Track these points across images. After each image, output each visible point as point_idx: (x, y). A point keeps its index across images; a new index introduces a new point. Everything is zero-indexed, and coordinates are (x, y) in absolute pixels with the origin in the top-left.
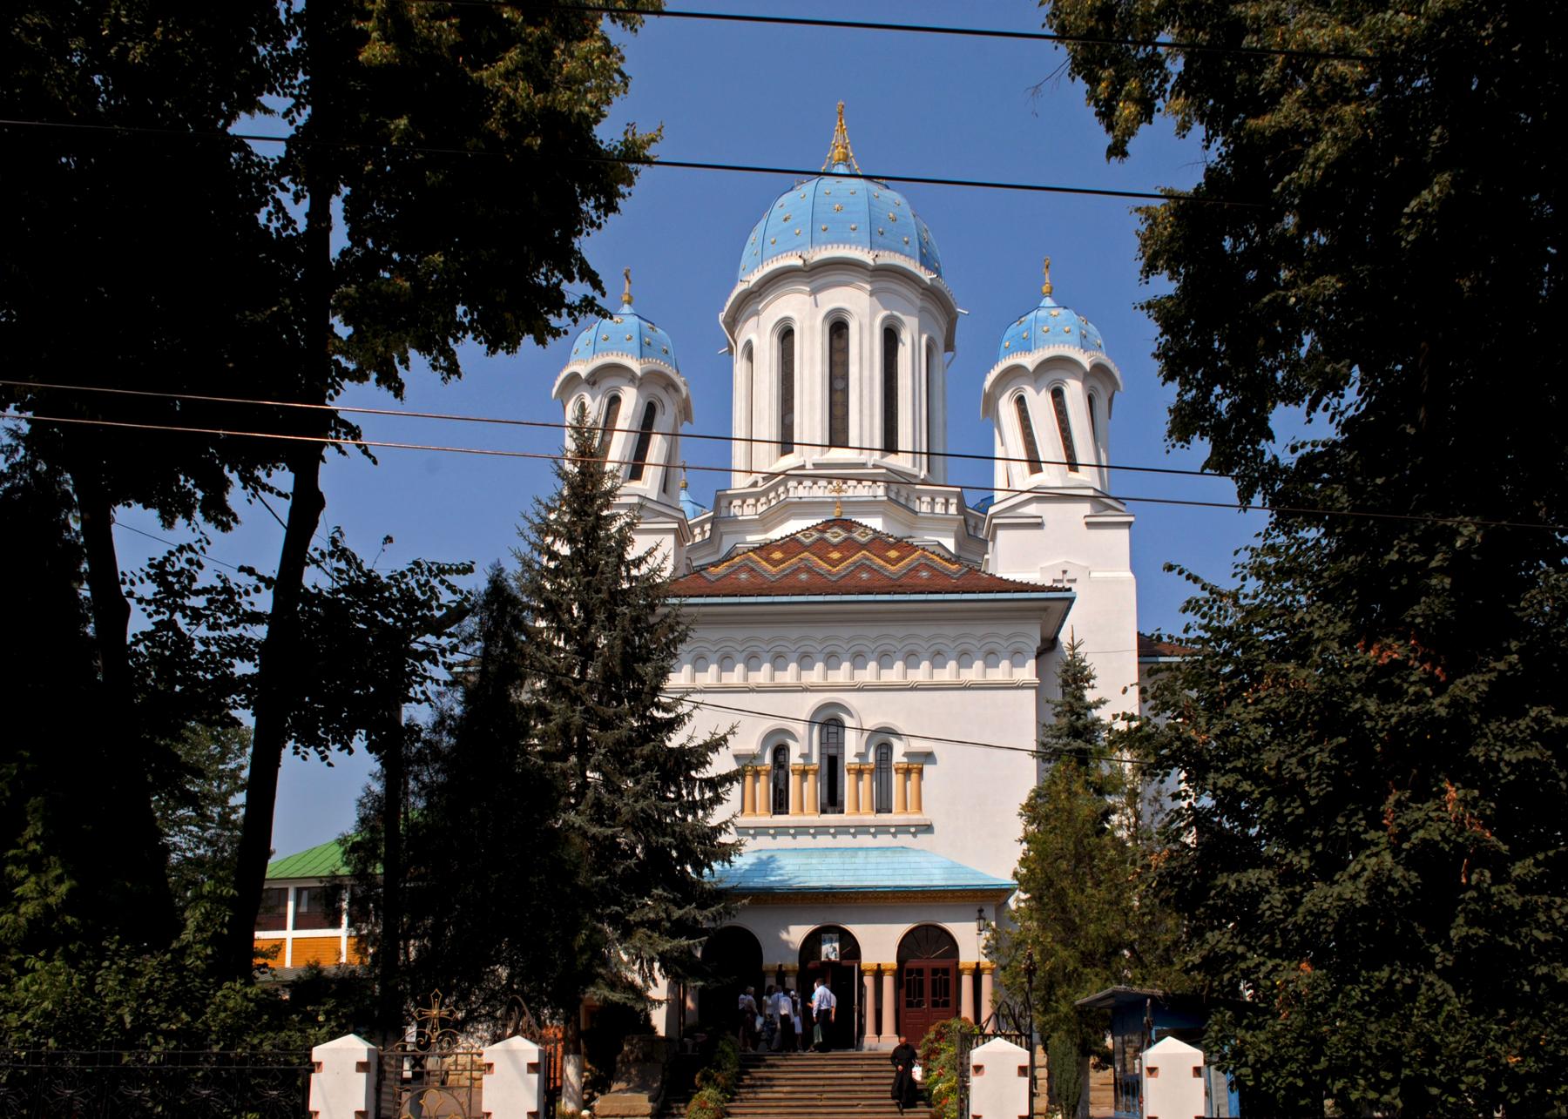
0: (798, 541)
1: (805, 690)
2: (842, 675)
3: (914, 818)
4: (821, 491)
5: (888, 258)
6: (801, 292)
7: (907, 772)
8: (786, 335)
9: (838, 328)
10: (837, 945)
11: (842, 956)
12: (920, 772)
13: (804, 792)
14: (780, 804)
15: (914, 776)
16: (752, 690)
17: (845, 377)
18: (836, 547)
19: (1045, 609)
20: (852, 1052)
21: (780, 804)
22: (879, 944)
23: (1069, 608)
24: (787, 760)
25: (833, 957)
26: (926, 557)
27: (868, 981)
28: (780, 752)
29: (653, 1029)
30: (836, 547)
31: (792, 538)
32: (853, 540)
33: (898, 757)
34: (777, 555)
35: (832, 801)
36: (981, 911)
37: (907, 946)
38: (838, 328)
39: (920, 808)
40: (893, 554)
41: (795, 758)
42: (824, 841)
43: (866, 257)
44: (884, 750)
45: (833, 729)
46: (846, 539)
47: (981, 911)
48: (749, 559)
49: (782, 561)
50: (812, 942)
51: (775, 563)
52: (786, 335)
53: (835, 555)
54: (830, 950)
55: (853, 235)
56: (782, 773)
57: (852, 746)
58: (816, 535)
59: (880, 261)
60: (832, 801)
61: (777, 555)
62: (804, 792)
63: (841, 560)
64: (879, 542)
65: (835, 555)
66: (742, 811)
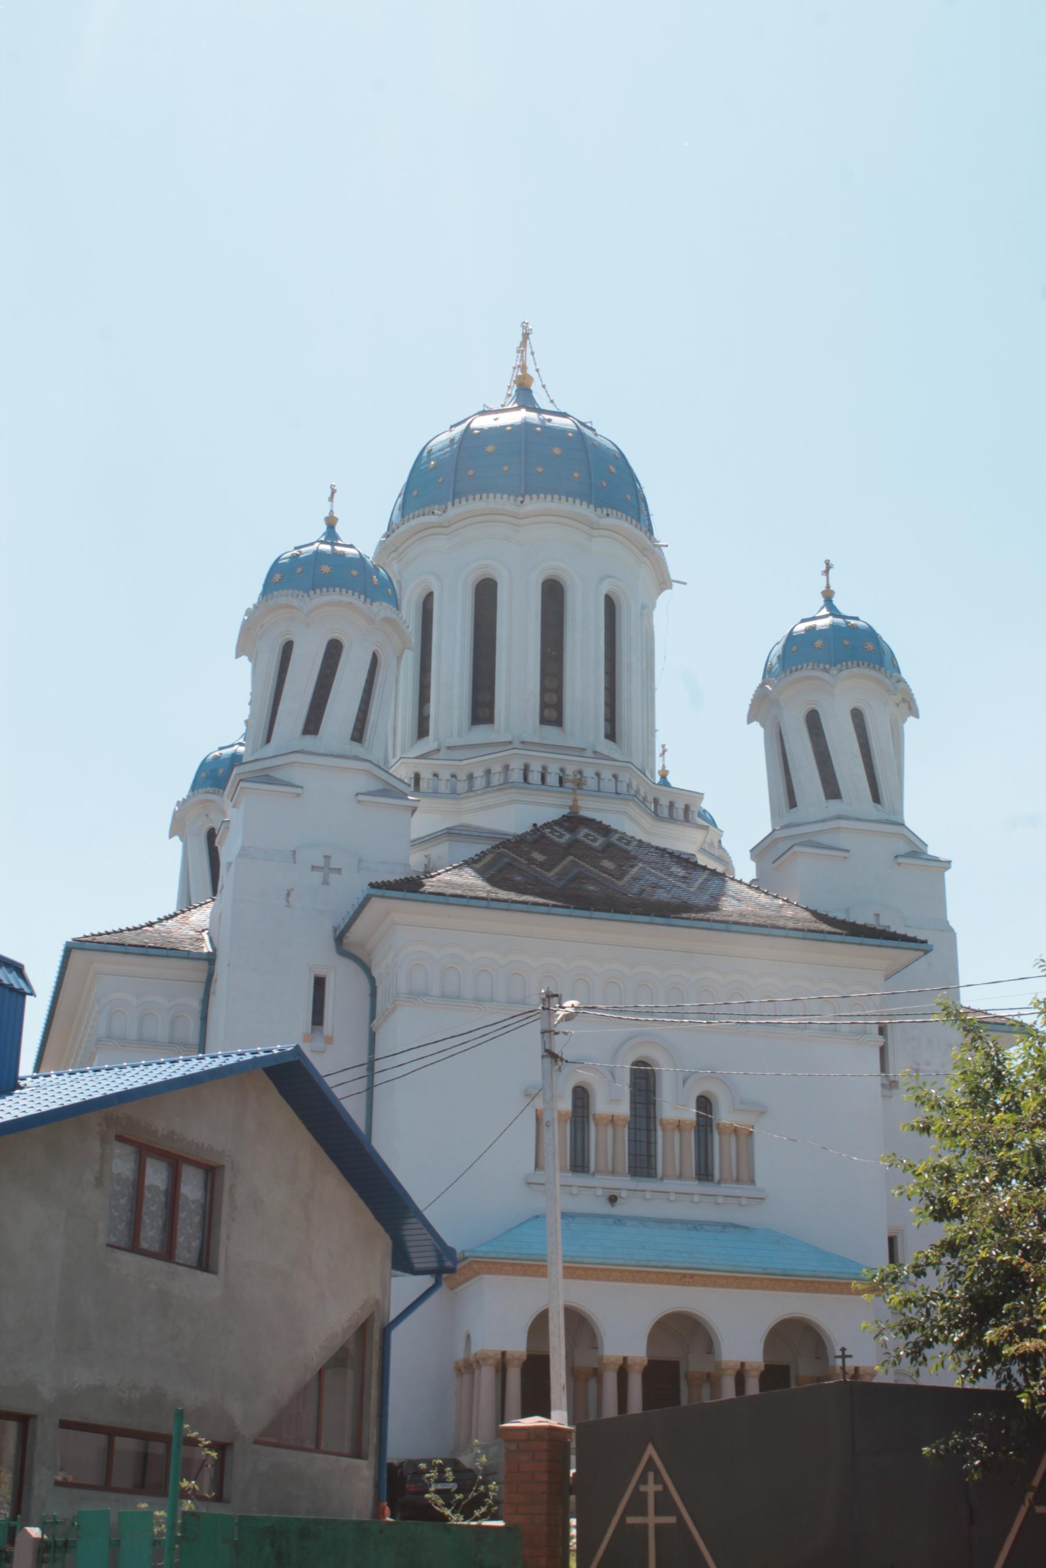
9: (553, 595)
33: (725, 1115)
38: (553, 595)
39: (752, 1181)
44: (704, 1103)
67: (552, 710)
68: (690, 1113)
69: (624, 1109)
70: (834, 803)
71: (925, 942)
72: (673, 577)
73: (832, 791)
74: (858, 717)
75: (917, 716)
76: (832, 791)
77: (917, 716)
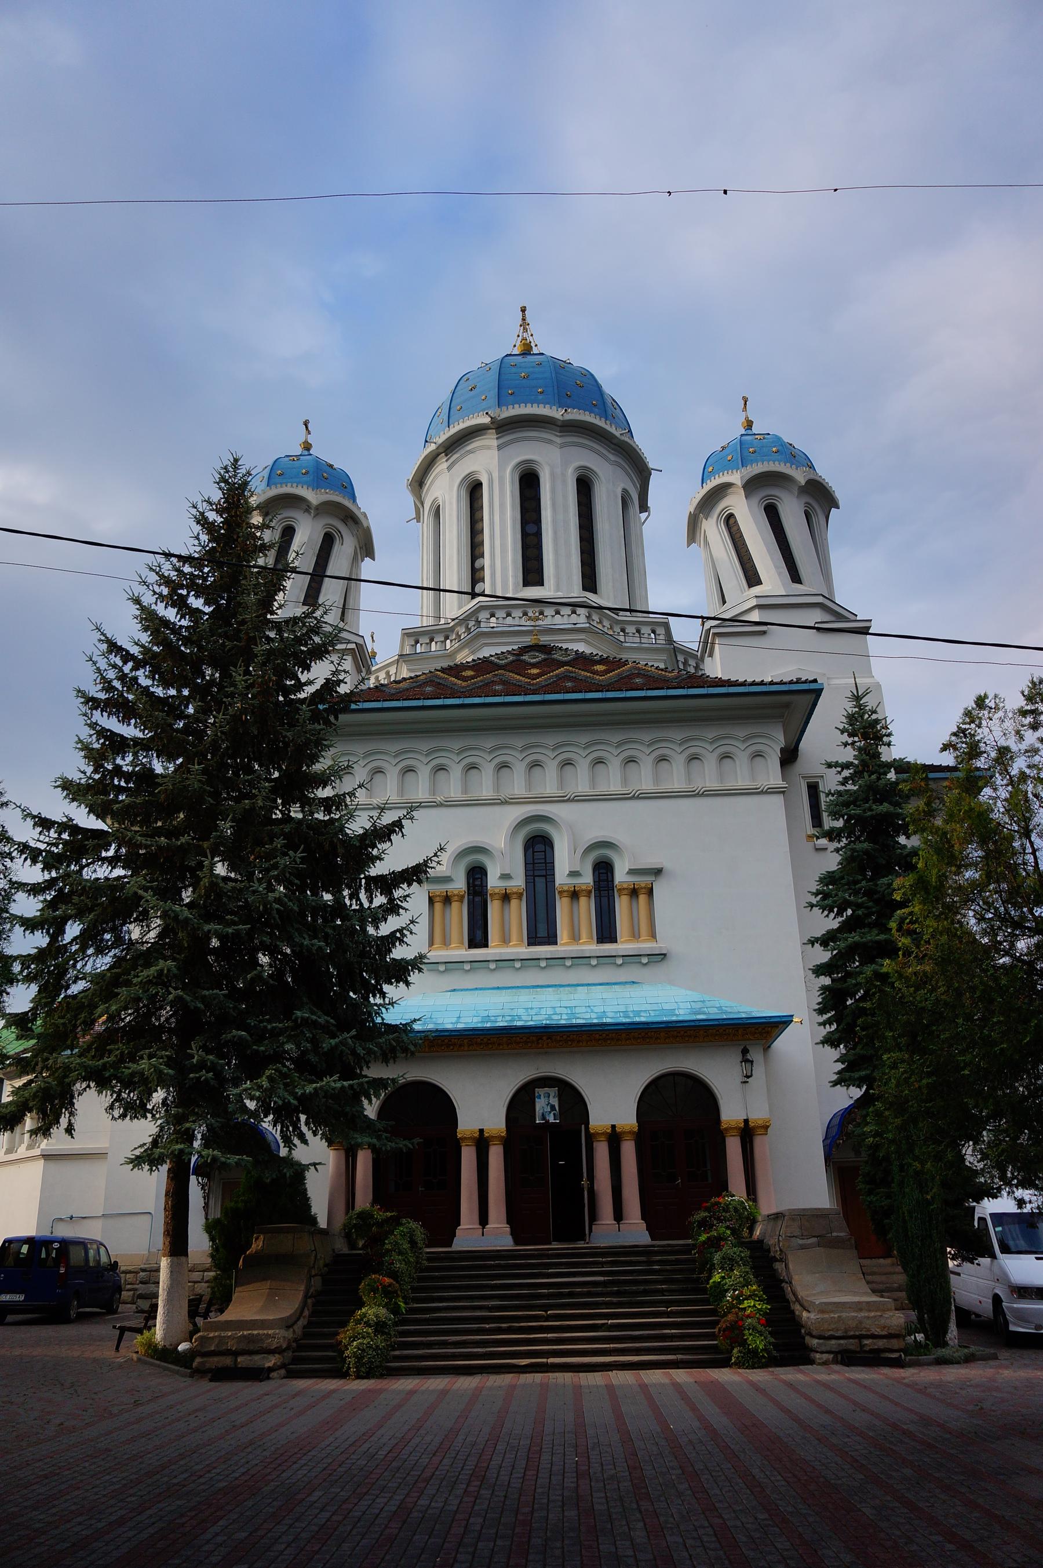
0: (491, 662)
1: (504, 803)
2: (549, 783)
3: (646, 946)
4: (517, 620)
5: (575, 415)
6: (489, 448)
7: (634, 893)
8: (474, 490)
9: (529, 483)
10: (555, 1102)
11: (563, 1113)
12: (650, 892)
13: (508, 922)
14: (478, 938)
15: (642, 898)
16: (440, 805)
17: (538, 521)
18: (534, 666)
19: (787, 705)
20: (581, 1244)
21: (478, 938)
22: (613, 1099)
23: (814, 705)
24: (484, 885)
25: (552, 1120)
26: (639, 669)
27: (602, 1151)
28: (477, 875)
29: (313, 1220)
30: (534, 666)
31: (485, 661)
32: (554, 660)
33: (621, 876)
34: (470, 673)
35: (541, 931)
36: (745, 1052)
37: (651, 1098)
38: (529, 483)
39: (653, 935)
40: (600, 668)
41: (493, 882)
42: (531, 977)
43: (557, 413)
44: (603, 869)
45: (540, 847)
46: (544, 660)
47: (745, 1052)
48: (437, 676)
49: (472, 677)
50: (520, 1104)
51: (465, 679)
52: (474, 490)
53: (535, 671)
54: (546, 1106)
55: (540, 397)
56: (478, 899)
57: (567, 864)
58: (511, 658)
59: (568, 417)
60: (541, 931)
61: (470, 673)
62: (508, 922)
63: (539, 675)
64: (582, 660)
65: (535, 671)
66: (431, 943)
67: (532, 570)
68: (587, 879)
69: (519, 882)
70: (757, 590)
71: (815, 681)
72: (651, 465)
73: (752, 578)
74: (772, 513)
75: (838, 508)
76: (752, 578)
77: (838, 508)
